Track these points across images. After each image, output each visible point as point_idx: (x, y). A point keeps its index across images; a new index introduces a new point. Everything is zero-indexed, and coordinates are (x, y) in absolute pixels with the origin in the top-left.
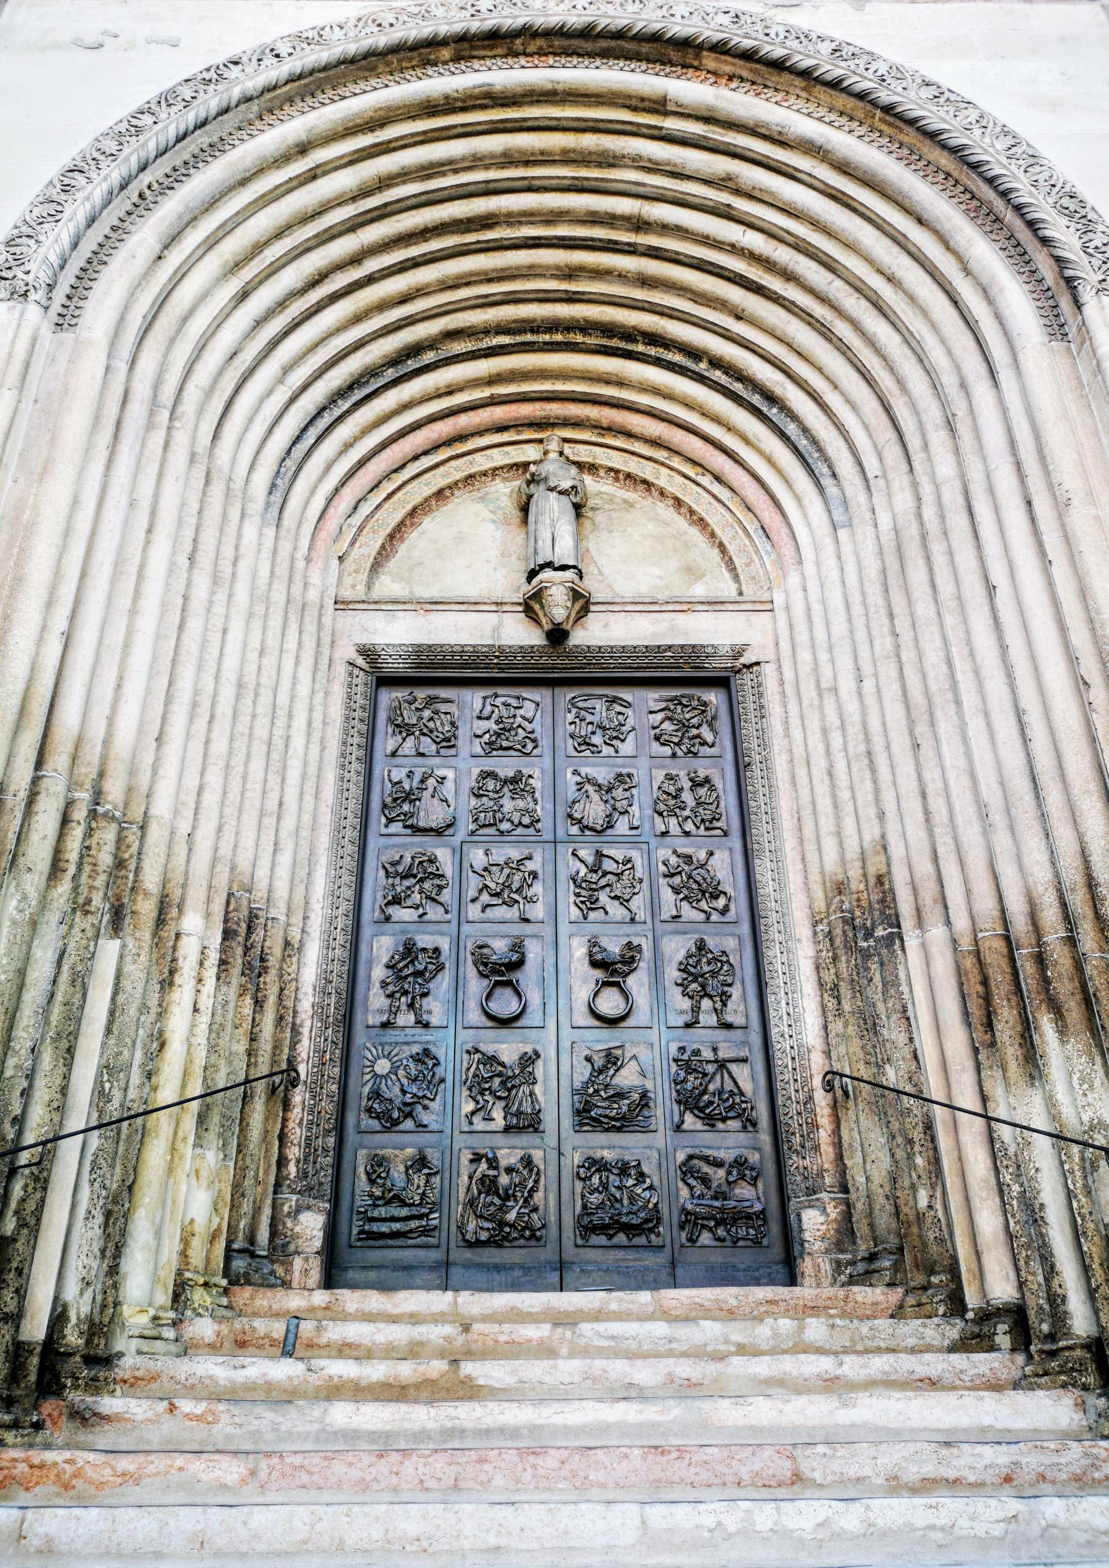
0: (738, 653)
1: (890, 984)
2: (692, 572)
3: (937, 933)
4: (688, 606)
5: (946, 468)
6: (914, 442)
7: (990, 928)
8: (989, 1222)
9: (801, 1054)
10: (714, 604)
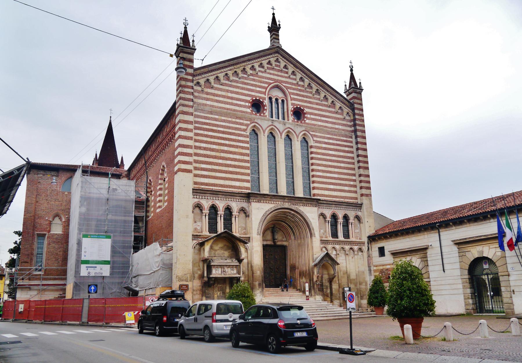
1: (295, 272)
2: (283, 238)
3: (298, 270)
5: (303, 242)
7: (301, 271)
8: (299, 285)
9: (288, 274)
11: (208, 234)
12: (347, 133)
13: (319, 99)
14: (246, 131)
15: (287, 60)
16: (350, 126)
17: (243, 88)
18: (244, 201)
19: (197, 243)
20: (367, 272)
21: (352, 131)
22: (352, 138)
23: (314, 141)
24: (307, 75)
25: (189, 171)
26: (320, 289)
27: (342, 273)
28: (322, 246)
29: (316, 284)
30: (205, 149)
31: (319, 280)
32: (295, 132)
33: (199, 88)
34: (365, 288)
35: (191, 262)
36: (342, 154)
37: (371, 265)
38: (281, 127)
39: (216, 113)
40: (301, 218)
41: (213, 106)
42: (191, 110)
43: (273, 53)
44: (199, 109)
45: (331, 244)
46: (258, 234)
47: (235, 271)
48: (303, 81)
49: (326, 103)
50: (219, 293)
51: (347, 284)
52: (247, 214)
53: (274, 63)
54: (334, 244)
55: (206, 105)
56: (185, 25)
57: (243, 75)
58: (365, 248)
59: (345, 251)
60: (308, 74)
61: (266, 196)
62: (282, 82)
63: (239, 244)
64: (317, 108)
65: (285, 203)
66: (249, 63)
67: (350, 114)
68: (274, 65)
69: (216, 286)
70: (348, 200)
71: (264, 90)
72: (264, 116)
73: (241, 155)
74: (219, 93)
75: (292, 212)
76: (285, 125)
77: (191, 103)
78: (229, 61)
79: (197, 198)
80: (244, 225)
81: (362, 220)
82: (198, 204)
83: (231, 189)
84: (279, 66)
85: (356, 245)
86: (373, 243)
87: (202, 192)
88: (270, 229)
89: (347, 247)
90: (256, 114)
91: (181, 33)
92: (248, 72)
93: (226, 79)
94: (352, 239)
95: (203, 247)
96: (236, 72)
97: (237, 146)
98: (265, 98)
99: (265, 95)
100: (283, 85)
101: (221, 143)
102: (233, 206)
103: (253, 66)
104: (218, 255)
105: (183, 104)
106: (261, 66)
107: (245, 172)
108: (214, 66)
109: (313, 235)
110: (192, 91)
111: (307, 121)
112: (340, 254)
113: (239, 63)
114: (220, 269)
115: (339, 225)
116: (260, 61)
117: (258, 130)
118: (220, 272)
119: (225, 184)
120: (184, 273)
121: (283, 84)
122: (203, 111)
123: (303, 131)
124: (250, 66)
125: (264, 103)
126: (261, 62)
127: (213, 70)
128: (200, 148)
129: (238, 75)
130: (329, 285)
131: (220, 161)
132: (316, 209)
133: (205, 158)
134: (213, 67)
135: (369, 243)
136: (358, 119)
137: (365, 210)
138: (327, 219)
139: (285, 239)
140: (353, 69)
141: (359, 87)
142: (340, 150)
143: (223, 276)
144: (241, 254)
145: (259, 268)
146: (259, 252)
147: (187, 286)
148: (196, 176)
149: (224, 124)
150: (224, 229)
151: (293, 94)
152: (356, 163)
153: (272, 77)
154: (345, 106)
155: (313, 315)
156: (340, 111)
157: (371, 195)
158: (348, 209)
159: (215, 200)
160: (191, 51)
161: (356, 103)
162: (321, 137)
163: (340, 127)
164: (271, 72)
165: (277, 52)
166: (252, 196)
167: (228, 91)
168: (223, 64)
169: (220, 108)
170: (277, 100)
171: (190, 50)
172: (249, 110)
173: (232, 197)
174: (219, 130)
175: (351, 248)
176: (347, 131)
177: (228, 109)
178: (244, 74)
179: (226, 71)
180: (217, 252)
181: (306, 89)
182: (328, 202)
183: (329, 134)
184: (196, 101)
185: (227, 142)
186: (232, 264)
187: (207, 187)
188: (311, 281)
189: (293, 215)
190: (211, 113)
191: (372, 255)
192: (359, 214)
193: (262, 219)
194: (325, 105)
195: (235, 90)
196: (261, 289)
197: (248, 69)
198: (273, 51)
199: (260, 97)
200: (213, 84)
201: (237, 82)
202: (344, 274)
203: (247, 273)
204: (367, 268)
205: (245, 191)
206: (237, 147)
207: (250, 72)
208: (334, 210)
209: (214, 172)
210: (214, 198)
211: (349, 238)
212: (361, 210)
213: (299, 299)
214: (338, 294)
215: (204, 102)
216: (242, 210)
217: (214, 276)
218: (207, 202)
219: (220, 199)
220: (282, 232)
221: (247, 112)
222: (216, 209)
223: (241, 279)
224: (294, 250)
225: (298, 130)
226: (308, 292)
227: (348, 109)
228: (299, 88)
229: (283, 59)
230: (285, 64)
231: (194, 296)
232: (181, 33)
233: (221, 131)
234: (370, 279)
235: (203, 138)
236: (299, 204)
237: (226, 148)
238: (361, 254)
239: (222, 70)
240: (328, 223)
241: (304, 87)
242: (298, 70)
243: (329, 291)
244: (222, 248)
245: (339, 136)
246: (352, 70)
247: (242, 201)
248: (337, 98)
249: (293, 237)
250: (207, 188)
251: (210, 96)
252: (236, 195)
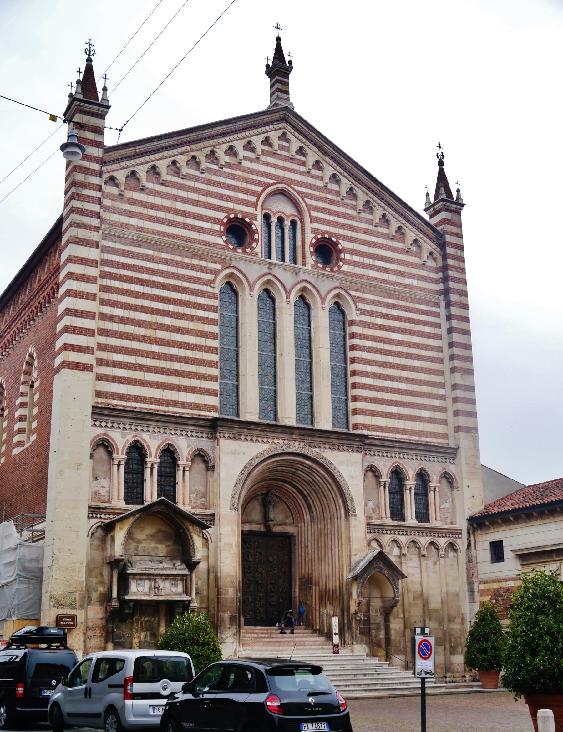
0: (293, 533)
1: (310, 592)
2: (287, 517)
3: (317, 588)
4: (286, 525)
5: (329, 527)
6: (326, 518)
8: (318, 621)
9: (296, 597)
10: (290, 525)
11: (122, 504)
12: (429, 296)
13: (371, 222)
14: (212, 285)
15: (305, 136)
16: (436, 282)
17: (208, 194)
18: (205, 435)
19: (99, 524)
20: (465, 596)
21: (439, 293)
22: (438, 305)
23: (358, 310)
24: (345, 170)
25: (86, 368)
26: (363, 630)
27: (411, 595)
28: (370, 536)
29: (356, 620)
30: (123, 320)
31: (361, 611)
32: (317, 291)
33: (114, 190)
34: (460, 630)
35: (85, 565)
36: (416, 340)
37: (475, 580)
38: (288, 279)
39: (149, 245)
40: (326, 476)
41: (143, 229)
42: (95, 236)
43: (275, 121)
44: (112, 235)
45: (389, 532)
46: (233, 507)
47: (180, 589)
48: (338, 182)
49: (386, 231)
50: (142, 636)
51: (422, 619)
52: (210, 464)
53: (276, 143)
54: (397, 533)
55: (127, 226)
56: (89, 55)
57: (209, 165)
58: (463, 544)
59: (419, 548)
60: (348, 167)
61: (252, 427)
62: (291, 182)
63: (191, 528)
64: (367, 241)
65: (292, 443)
66: (223, 139)
67: (437, 255)
68: (276, 147)
69: (138, 620)
70: (428, 439)
71: (253, 199)
72: (251, 254)
73: (201, 336)
74: (158, 201)
75: (308, 462)
76: (296, 274)
77: (95, 222)
78: (181, 135)
79: (101, 426)
80: (202, 489)
81: (457, 483)
82: (103, 440)
83: (176, 410)
84: (288, 149)
85: (444, 535)
86: (479, 532)
87: (113, 413)
88: (260, 497)
89: (424, 541)
90: (234, 250)
91: (80, 72)
92: (220, 159)
93: (172, 172)
94: (434, 523)
95: (112, 534)
96: (194, 158)
97: (193, 316)
98: (256, 216)
99: (256, 209)
100: (295, 190)
101: (158, 309)
102: (179, 447)
103: (231, 147)
104: (144, 551)
105: (78, 224)
106: (249, 146)
107: (208, 373)
108: (148, 145)
109: (351, 513)
110: (98, 195)
111: (345, 268)
112: (407, 554)
113: (201, 139)
114: (147, 583)
115: (408, 492)
116: (248, 137)
117: (237, 283)
118: (146, 590)
119: (164, 398)
120: (69, 590)
121: (296, 187)
122: (120, 238)
123: (336, 288)
124: (225, 147)
125: (253, 226)
126: (249, 139)
127: (146, 153)
128: (111, 318)
129: (198, 164)
130: (383, 622)
131: (155, 348)
132: (358, 456)
133: (122, 340)
134: (145, 146)
135: (471, 532)
136: (453, 267)
137: (463, 461)
138: (381, 480)
139: (290, 520)
140: (444, 160)
141: (455, 198)
142: (414, 331)
143: (153, 597)
144: (194, 551)
145: (232, 582)
146: (234, 547)
147: (73, 618)
148: (100, 378)
149: (165, 268)
150: (159, 495)
151: (316, 209)
152: (447, 360)
153: (271, 170)
154: (425, 238)
155: (347, 686)
156: (414, 248)
157: (476, 429)
158: (427, 459)
159: (141, 433)
160: (98, 110)
161: (448, 233)
162: (373, 303)
163: (415, 283)
164: (271, 160)
165: (284, 120)
166: (221, 426)
167: (175, 198)
168: (166, 141)
169: (159, 233)
170: (280, 220)
171: (97, 107)
172: (220, 241)
173: (178, 426)
174: (153, 281)
175: (432, 543)
176: (430, 291)
177: (174, 237)
178: (212, 163)
179: (173, 156)
180: (141, 546)
181: (343, 199)
182: (386, 443)
183: (390, 296)
184: (107, 218)
185: (171, 308)
186: (173, 573)
187: (124, 403)
188: (345, 614)
189: (310, 467)
190: (139, 243)
191: (476, 557)
192: (452, 469)
193: (242, 474)
194: (383, 235)
195: (191, 196)
196: (234, 627)
197: (220, 153)
198: (276, 116)
199: (246, 214)
200: (144, 182)
201: (196, 179)
202: (415, 598)
203: (205, 593)
204: (466, 587)
205: (207, 413)
206: (192, 318)
207: (224, 158)
208: (398, 460)
209: (140, 370)
210: (139, 428)
211: (427, 520)
212: (455, 461)
213: (318, 652)
214: (402, 642)
215: (124, 219)
216: (199, 454)
217: (134, 598)
218: (124, 436)
219: (151, 429)
220: (284, 504)
221: (215, 245)
222: (143, 452)
223: (191, 605)
224: (310, 544)
225: (325, 285)
226: (337, 636)
227: (432, 244)
228: (329, 196)
229: (297, 134)
230: (301, 144)
231: (88, 640)
232: (80, 72)
233: (159, 283)
234: (471, 610)
235: (119, 296)
236: (322, 446)
237: (167, 321)
238: (454, 557)
239: (165, 154)
240: (385, 487)
241: (339, 196)
242: (327, 159)
243: (382, 635)
244: (152, 537)
245: (411, 302)
246: (441, 163)
247: (200, 435)
248: (408, 221)
249: (307, 517)
250: (124, 406)
251: (138, 207)
252: (186, 421)
